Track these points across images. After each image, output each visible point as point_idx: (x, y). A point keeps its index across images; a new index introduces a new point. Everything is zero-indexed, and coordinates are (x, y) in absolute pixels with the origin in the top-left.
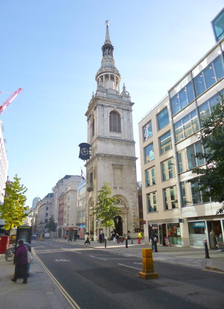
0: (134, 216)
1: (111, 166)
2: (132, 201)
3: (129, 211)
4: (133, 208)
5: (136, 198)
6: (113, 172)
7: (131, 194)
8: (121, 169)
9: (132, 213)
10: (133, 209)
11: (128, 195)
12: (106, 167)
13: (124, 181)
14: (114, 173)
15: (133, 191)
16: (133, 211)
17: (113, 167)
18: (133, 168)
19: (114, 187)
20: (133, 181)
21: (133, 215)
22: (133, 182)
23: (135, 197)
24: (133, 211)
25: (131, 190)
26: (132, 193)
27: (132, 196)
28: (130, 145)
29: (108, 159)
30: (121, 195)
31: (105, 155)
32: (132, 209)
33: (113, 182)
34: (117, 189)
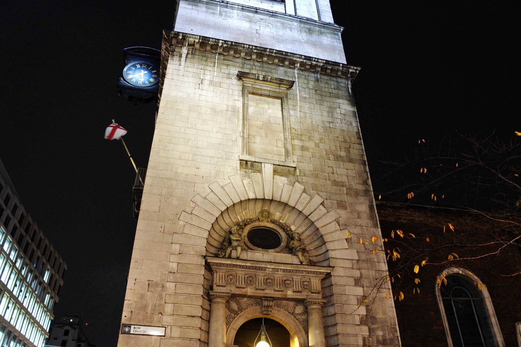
0: (368, 320)
1: (235, 81)
2: (346, 234)
3: (339, 329)
4: (357, 274)
5: (369, 223)
6: (239, 104)
7: (341, 205)
8: (281, 99)
9: (354, 301)
10: (358, 282)
11: (322, 204)
12: (206, 82)
13: (296, 142)
14: (245, 107)
15: (349, 189)
16: (359, 291)
17: (244, 88)
18: (341, 101)
19: (244, 163)
20: (348, 150)
21: (362, 311)
22: (343, 154)
23: (365, 221)
24: (359, 291)
25: (336, 183)
26: (346, 198)
27: (343, 213)
28: (321, 33)
29: (222, 57)
30: (286, 205)
31: (204, 41)
32: (352, 282)
33: (240, 140)
34: (260, 171)
